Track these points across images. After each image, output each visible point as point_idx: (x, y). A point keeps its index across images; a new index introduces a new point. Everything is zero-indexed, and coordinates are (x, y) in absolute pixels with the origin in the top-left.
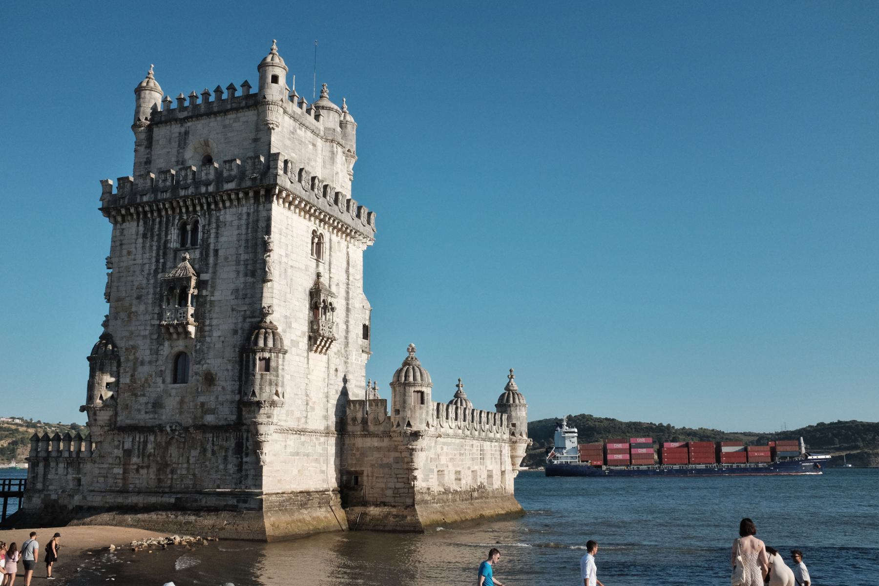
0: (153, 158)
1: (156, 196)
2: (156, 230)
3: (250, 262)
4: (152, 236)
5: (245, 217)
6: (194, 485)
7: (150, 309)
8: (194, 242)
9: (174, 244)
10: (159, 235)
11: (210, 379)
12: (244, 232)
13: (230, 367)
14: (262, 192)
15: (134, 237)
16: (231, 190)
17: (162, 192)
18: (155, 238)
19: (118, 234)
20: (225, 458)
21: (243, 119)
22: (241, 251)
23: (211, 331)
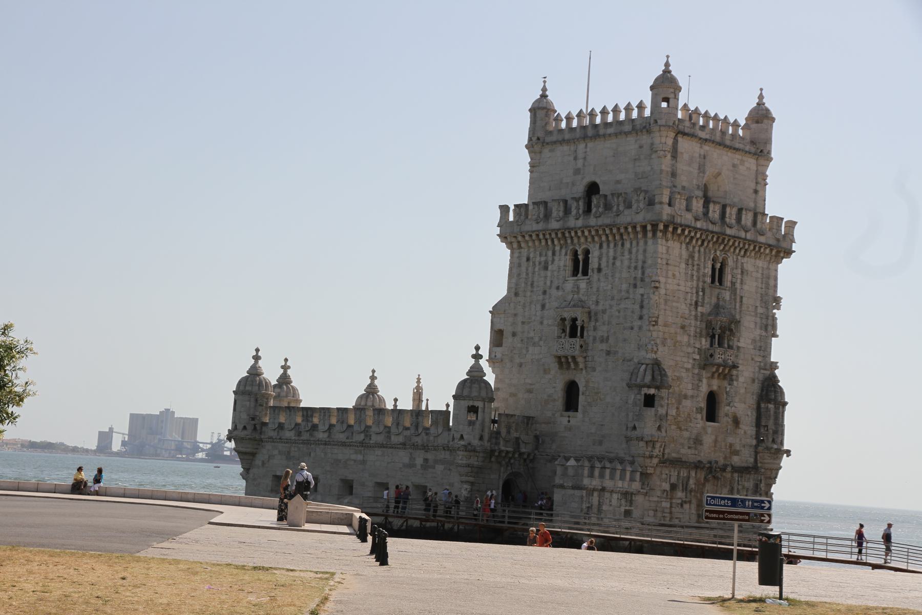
0: (679, 172)
2: (696, 259)
3: (764, 317)
5: (760, 271)
7: (692, 342)
9: (709, 280)
11: (736, 422)
12: (760, 286)
13: (749, 413)
14: (782, 255)
16: (765, 244)
17: (713, 223)
18: (695, 268)
19: (664, 250)
21: (747, 164)
23: (737, 376)
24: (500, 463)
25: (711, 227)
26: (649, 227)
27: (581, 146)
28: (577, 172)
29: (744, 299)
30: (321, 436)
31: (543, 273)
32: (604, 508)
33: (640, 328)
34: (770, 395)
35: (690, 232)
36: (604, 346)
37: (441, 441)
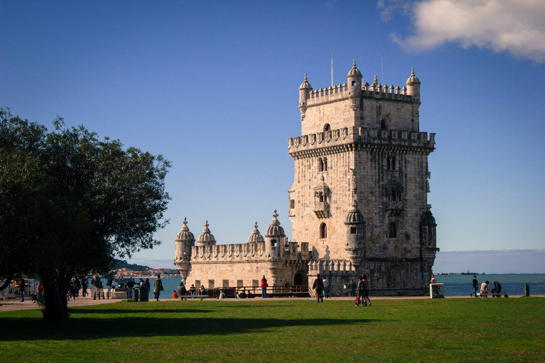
0: (365, 116)
1: (381, 142)
4: (375, 161)
6: (404, 286)
7: (378, 199)
8: (394, 168)
9: (385, 168)
10: (379, 161)
11: (408, 236)
14: (428, 151)
15: (366, 160)
16: (416, 147)
20: (416, 273)
21: (405, 107)
22: (417, 176)
23: (406, 214)
24: (292, 266)
25: (383, 142)
26: (349, 146)
27: (322, 106)
28: (321, 119)
29: (408, 176)
30: (214, 259)
31: (309, 171)
32: (332, 284)
33: (349, 195)
34: (427, 222)
35: (370, 146)
36: (335, 205)
37: (262, 258)
